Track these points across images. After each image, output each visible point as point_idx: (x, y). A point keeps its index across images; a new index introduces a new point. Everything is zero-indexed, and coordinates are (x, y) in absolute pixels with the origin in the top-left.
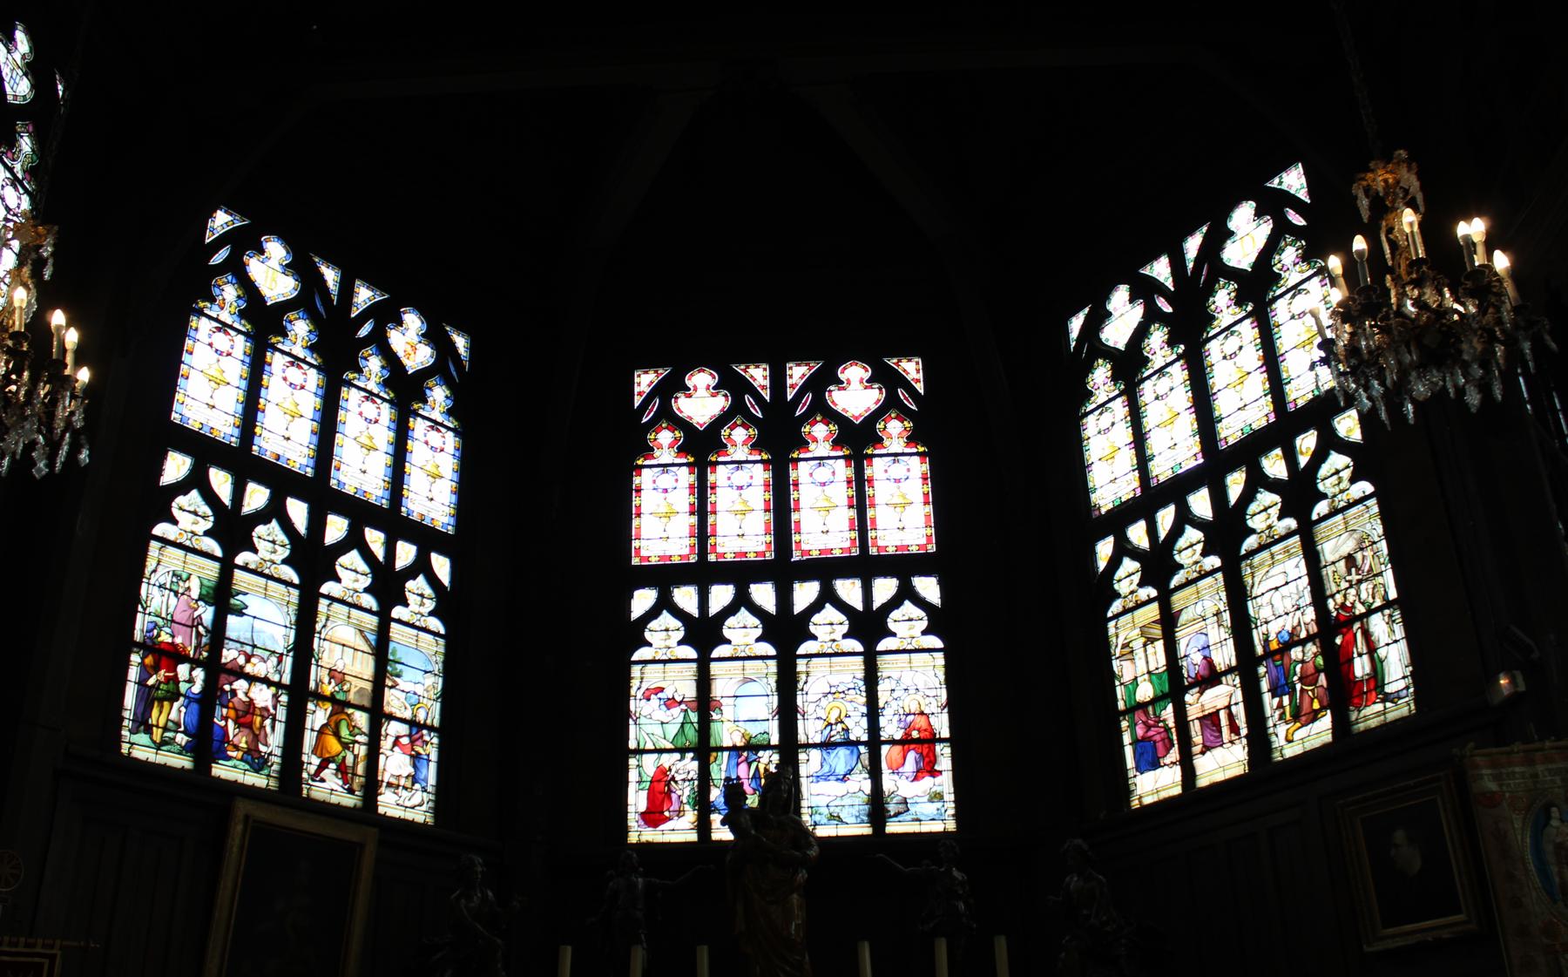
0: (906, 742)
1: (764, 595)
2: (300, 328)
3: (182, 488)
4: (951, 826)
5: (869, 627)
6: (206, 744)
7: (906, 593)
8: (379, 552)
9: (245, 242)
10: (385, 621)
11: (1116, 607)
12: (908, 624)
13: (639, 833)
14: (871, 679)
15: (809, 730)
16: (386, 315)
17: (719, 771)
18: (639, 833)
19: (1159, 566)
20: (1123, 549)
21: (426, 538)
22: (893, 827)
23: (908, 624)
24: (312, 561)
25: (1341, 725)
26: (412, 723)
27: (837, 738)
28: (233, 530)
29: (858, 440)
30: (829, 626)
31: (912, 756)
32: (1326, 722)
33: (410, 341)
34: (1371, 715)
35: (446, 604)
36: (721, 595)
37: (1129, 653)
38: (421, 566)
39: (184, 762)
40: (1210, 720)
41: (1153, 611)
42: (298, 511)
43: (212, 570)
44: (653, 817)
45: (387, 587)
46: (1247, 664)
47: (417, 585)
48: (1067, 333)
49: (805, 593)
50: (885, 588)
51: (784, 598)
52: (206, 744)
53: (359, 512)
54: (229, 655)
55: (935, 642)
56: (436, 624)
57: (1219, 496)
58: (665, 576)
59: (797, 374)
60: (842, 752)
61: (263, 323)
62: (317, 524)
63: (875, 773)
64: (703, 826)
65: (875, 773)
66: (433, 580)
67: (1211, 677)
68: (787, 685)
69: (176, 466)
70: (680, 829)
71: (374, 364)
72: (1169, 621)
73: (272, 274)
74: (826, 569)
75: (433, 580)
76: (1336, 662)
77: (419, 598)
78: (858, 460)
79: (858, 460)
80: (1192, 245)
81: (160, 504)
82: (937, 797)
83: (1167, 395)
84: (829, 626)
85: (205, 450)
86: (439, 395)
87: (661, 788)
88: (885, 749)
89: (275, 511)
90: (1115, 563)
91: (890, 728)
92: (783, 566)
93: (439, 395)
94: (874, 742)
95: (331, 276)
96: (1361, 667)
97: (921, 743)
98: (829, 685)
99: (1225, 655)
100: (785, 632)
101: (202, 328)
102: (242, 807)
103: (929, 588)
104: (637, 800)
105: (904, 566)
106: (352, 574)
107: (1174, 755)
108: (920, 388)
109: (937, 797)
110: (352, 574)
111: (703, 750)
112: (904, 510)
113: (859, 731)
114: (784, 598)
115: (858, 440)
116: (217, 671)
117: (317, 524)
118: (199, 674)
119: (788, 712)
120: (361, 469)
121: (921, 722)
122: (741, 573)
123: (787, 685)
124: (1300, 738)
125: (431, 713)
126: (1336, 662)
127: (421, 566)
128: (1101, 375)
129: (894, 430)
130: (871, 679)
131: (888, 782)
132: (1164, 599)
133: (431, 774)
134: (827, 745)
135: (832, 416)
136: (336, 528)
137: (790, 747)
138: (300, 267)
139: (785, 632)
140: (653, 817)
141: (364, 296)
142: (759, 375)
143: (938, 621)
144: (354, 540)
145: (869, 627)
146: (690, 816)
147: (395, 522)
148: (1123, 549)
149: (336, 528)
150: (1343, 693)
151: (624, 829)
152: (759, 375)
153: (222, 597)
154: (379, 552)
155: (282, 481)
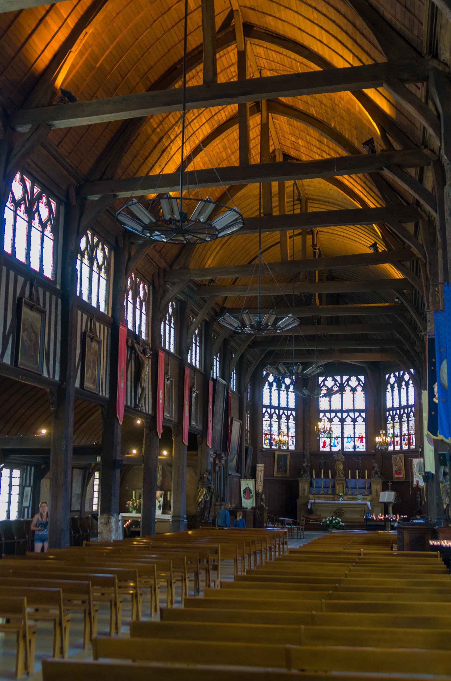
0: (359, 438)
1: (339, 415)
2: (275, 384)
3: (265, 413)
4: (365, 450)
5: (354, 420)
6: (271, 444)
7: (360, 415)
8: (286, 414)
9: (268, 375)
10: (288, 423)
11: (388, 422)
12: (360, 420)
13: (322, 449)
14: (354, 428)
15: (345, 435)
17: (333, 441)
18: (322, 449)
19: (393, 419)
20: (389, 414)
21: (292, 410)
22: (357, 450)
23: (360, 420)
24: (279, 417)
25: (409, 447)
26: (292, 437)
27: (349, 437)
28: (271, 416)
29: (354, 390)
30: (348, 420)
31: (360, 440)
32: (407, 446)
33: (288, 381)
34: (412, 447)
36: (333, 415)
37: (389, 430)
38: (291, 414)
39: (269, 447)
40: (397, 442)
41: (392, 425)
42: (277, 411)
43: (269, 422)
44: (324, 447)
45: (288, 418)
46: (401, 436)
47: (291, 417)
48: (385, 377)
49: (345, 415)
50: (357, 414)
52: (271, 444)
53: (284, 409)
54: (272, 433)
55: (364, 423)
56: (294, 422)
57: (400, 412)
58: (325, 411)
59: (345, 378)
60: (350, 439)
61: (271, 385)
62: (279, 412)
63: (354, 442)
64: (331, 449)
65: (354, 442)
66: (293, 416)
67: (397, 436)
68: (342, 428)
69: (264, 410)
70: (327, 449)
72: (393, 427)
74: (348, 411)
75: (293, 416)
76: (409, 439)
78: (354, 394)
79: (354, 394)
80: (402, 373)
81: (263, 416)
82: (363, 446)
83: (396, 393)
84: (348, 420)
85: (267, 407)
87: (324, 443)
88: (356, 439)
89: (275, 412)
90: (388, 416)
91: (357, 436)
92: (342, 411)
93: (292, 387)
94: (354, 438)
96: (411, 441)
97: (361, 438)
98: (348, 430)
99: (399, 434)
100: (342, 421)
101: (264, 390)
102: (277, 453)
103: (363, 415)
104: (321, 445)
105: (360, 411)
106: (284, 417)
107: (393, 445)
108: (364, 382)
109: (363, 446)
110: (284, 417)
111: (330, 438)
112: (361, 404)
113: (352, 436)
115: (354, 390)
116: (271, 435)
117: (279, 412)
118: (269, 436)
119: (342, 433)
121: (361, 435)
122: (336, 411)
123: (342, 428)
124: (405, 448)
125: (294, 434)
126: (409, 439)
127: (291, 414)
128: (389, 386)
129: (359, 389)
130: (354, 428)
131: (356, 443)
132: (393, 423)
133: (294, 443)
134: (348, 438)
135: (350, 386)
136: (281, 412)
137: (342, 438)
139: (342, 421)
140: (324, 447)
142: (338, 378)
143: (365, 420)
144: (284, 413)
145: (354, 420)
146: (329, 447)
147: (288, 409)
148: (389, 414)
149: (281, 412)
150: (410, 444)
151: (320, 449)
152: (338, 378)
153: (270, 426)
154: (286, 414)
155: (275, 408)
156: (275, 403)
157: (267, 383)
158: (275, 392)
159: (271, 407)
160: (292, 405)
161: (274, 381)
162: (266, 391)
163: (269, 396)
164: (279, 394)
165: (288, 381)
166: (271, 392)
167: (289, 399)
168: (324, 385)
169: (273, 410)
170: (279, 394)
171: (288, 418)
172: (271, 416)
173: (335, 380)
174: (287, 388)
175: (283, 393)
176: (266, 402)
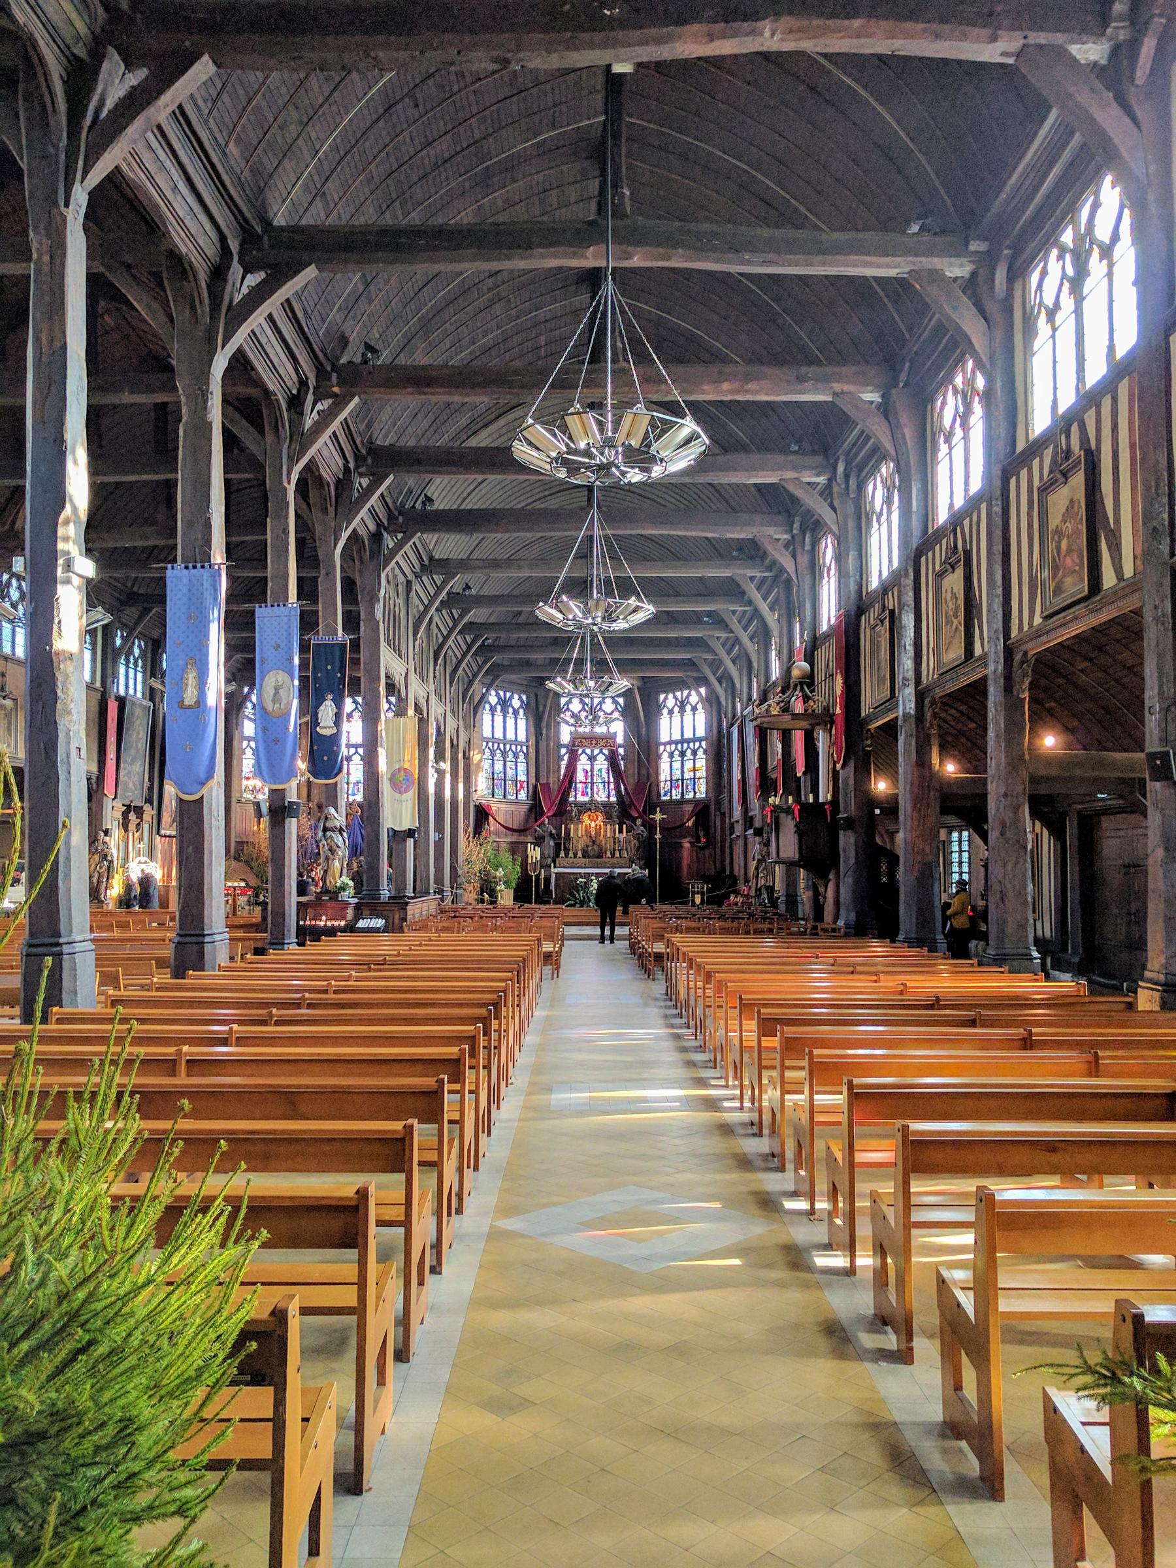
16: (512, 697)
24: (504, 754)
28: (493, 753)
33: (516, 703)
35: (526, 756)
45: (516, 755)
51: (592, 752)
61: (493, 710)
71: (511, 710)
73: (493, 699)
77: (521, 758)
86: (521, 711)
95: (502, 693)
114: (592, 752)
120: (510, 736)
136: (508, 747)
137: (592, 783)
138: (498, 695)
141: (508, 694)
156: (499, 734)
157: (487, 706)
158: (499, 719)
159: (493, 739)
160: (522, 737)
161: (498, 703)
162: (486, 717)
163: (490, 724)
164: (505, 722)
165: (516, 703)
166: (493, 721)
167: (519, 729)
168: (568, 709)
169: (496, 745)
170: (505, 722)
171: (516, 755)
172: (493, 753)
173: (583, 703)
174: (516, 713)
175: (510, 721)
176: (487, 733)
